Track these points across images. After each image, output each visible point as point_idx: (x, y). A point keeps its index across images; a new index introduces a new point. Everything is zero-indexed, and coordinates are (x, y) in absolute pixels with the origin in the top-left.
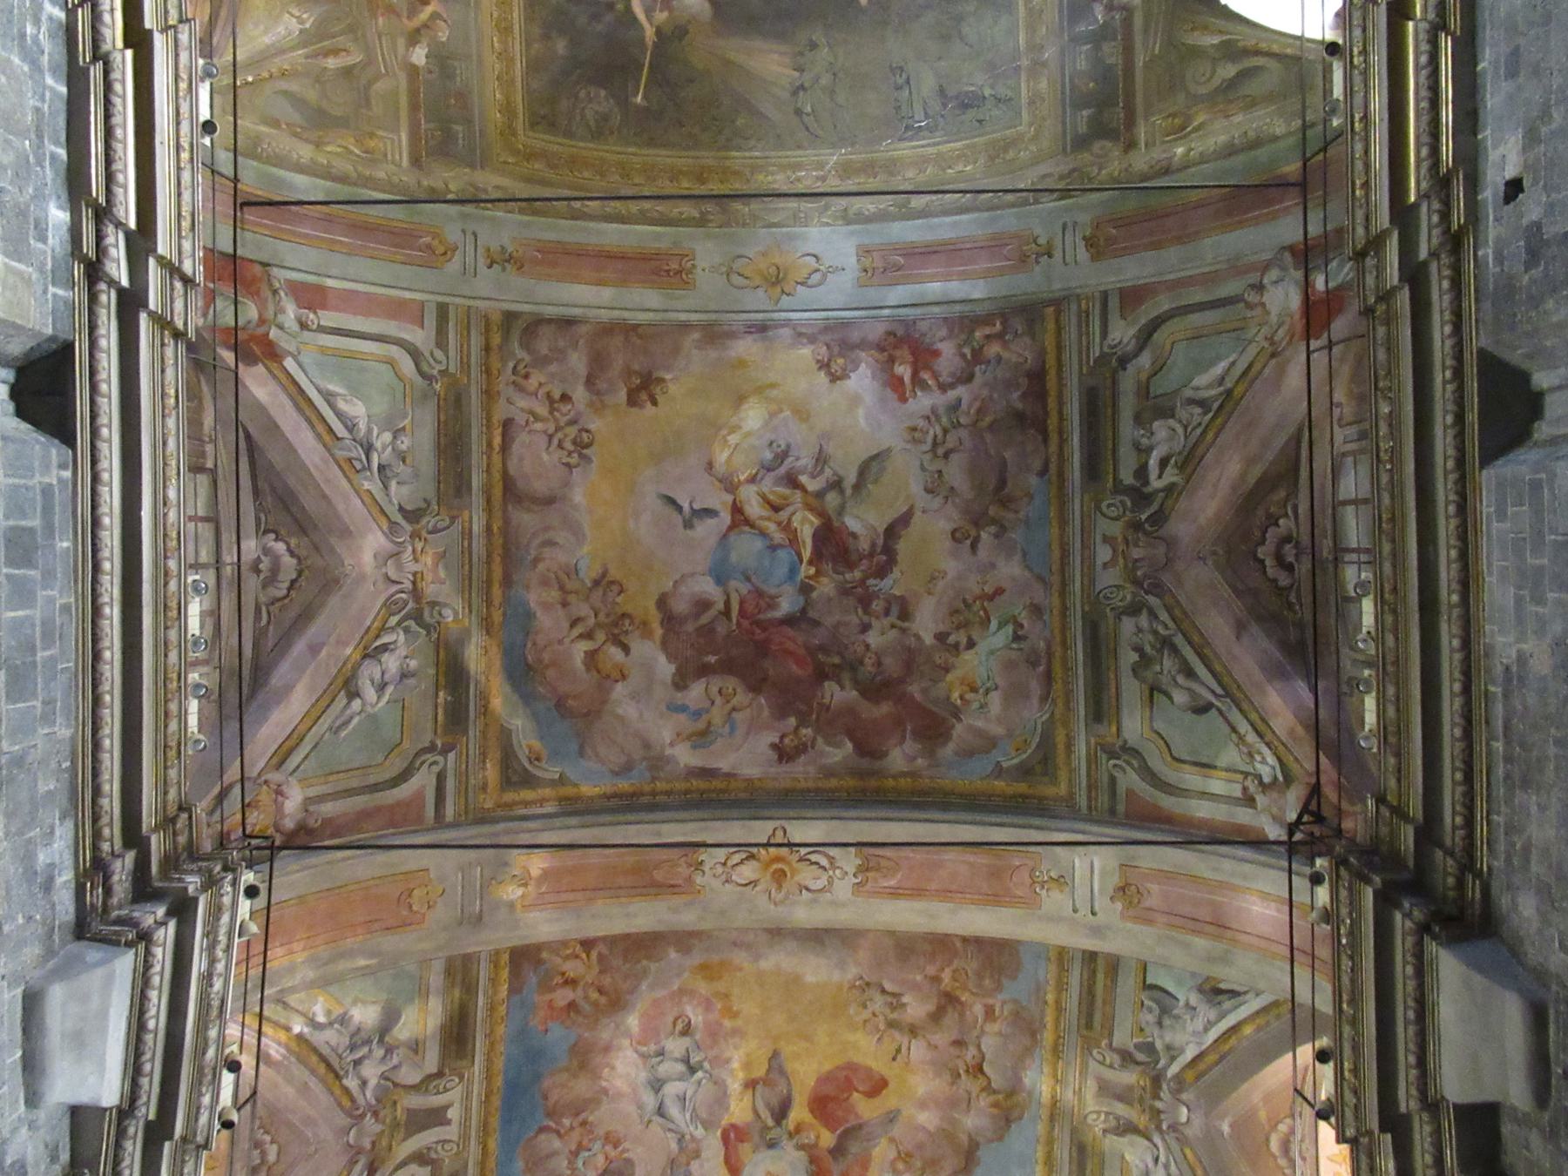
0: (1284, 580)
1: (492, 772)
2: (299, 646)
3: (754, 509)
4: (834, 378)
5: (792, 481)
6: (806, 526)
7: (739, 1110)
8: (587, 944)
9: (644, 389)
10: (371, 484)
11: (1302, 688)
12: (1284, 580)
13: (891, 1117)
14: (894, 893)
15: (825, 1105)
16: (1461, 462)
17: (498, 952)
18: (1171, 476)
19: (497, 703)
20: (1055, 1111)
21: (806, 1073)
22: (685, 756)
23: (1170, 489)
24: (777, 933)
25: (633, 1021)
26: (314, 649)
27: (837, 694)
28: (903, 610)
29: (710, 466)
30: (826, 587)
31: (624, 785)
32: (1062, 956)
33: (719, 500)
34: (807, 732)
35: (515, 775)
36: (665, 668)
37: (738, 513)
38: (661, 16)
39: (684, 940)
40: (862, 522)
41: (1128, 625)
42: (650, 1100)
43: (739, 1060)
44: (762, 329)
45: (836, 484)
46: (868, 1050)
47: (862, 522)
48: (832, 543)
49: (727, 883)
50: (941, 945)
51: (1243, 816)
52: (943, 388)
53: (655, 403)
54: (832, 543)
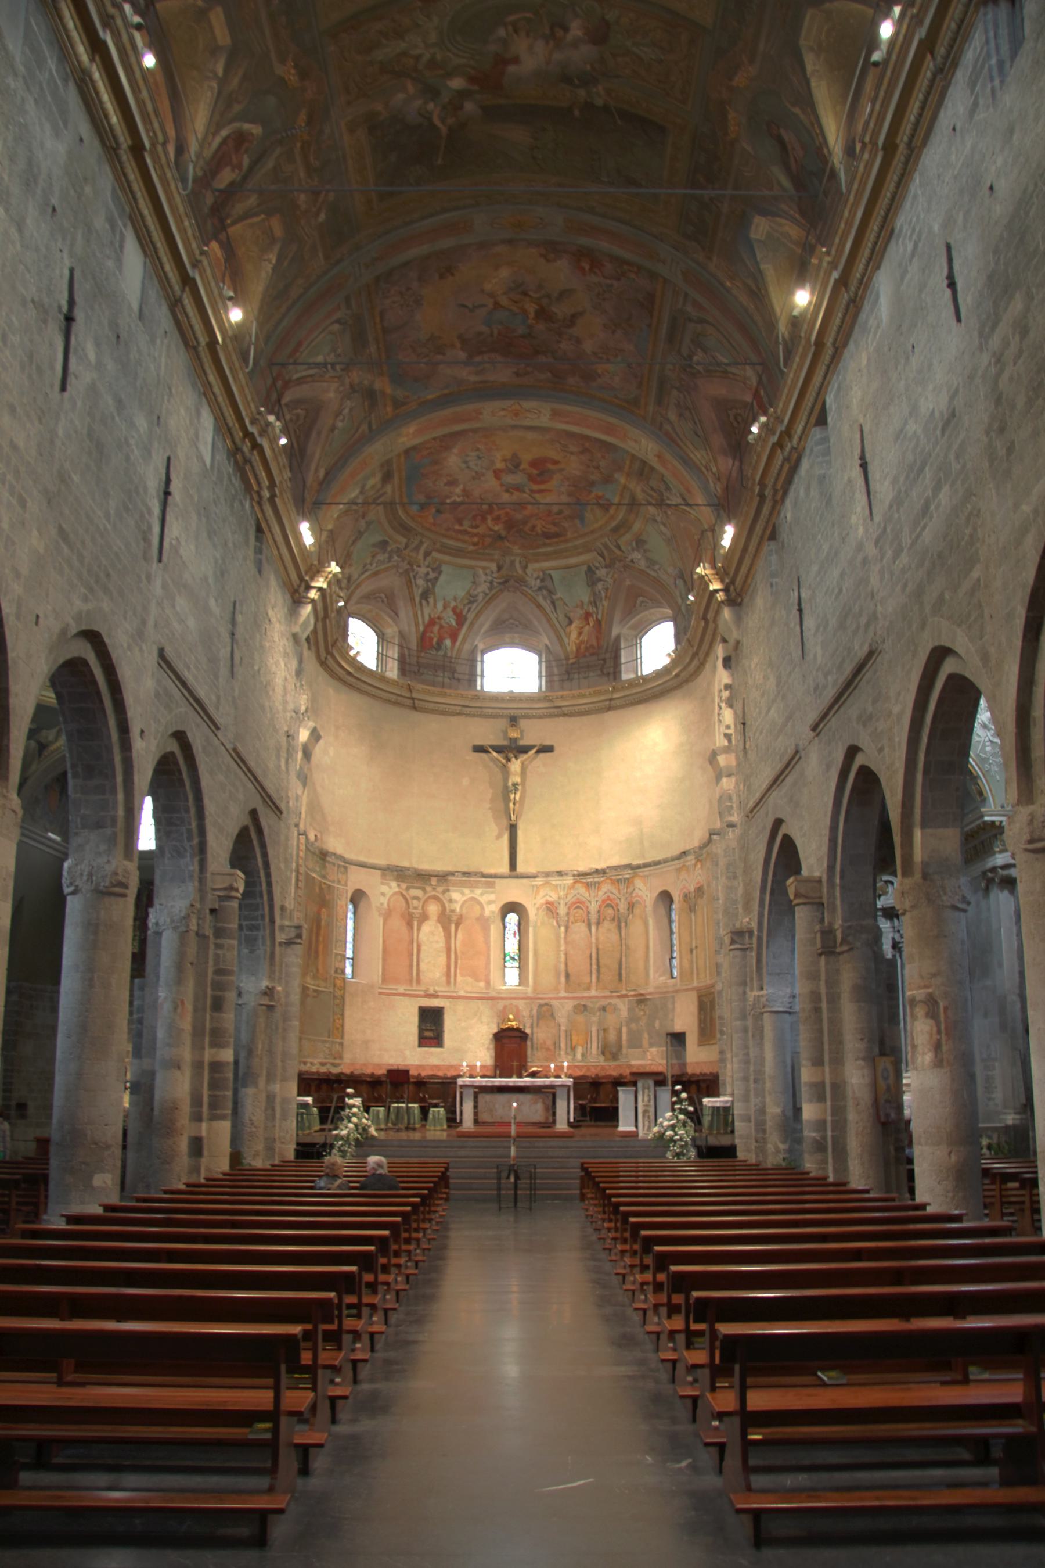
0: (735, 424)
1: (389, 409)
2: (314, 435)
3: (504, 301)
4: (548, 261)
5: (525, 294)
6: (531, 308)
7: (500, 465)
8: (434, 439)
9: (449, 271)
10: (332, 373)
11: (730, 461)
12: (735, 424)
13: (562, 470)
14: (567, 423)
15: (534, 464)
16: (762, 538)
17: (399, 456)
18: (700, 368)
19: (389, 391)
20: (625, 487)
21: (526, 457)
22: (473, 378)
23: (699, 372)
24: (514, 427)
25: (455, 451)
26: (319, 433)
27: (542, 359)
28: (578, 341)
29: (482, 291)
30: (541, 327)
31: (446, 391)
32: (633, 457)
33: (490, 303)
34: (529, 369)
35: (397, 404)
36: (462, 355)
37: (497, 305)
38: (450, 121)
39: (475, 431)
40: (561, 310)
41: (675, 392)
42: (464, 466)
43: (498, 456)
44: (510, 242)
45: (549, 296)
46: (552, 454)
47: (561, 310)
48: (543, 314)
49: (493, 413)
50: (587, 438)
51: (703, 469)
52: (605, 277)
53: (452, 275)
54: (543, 314)
